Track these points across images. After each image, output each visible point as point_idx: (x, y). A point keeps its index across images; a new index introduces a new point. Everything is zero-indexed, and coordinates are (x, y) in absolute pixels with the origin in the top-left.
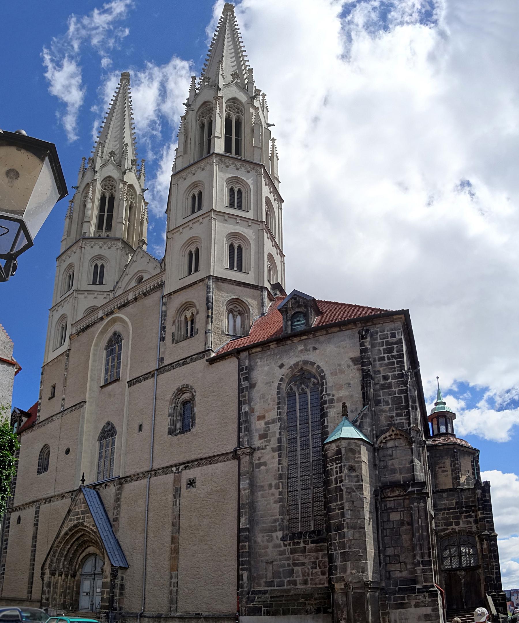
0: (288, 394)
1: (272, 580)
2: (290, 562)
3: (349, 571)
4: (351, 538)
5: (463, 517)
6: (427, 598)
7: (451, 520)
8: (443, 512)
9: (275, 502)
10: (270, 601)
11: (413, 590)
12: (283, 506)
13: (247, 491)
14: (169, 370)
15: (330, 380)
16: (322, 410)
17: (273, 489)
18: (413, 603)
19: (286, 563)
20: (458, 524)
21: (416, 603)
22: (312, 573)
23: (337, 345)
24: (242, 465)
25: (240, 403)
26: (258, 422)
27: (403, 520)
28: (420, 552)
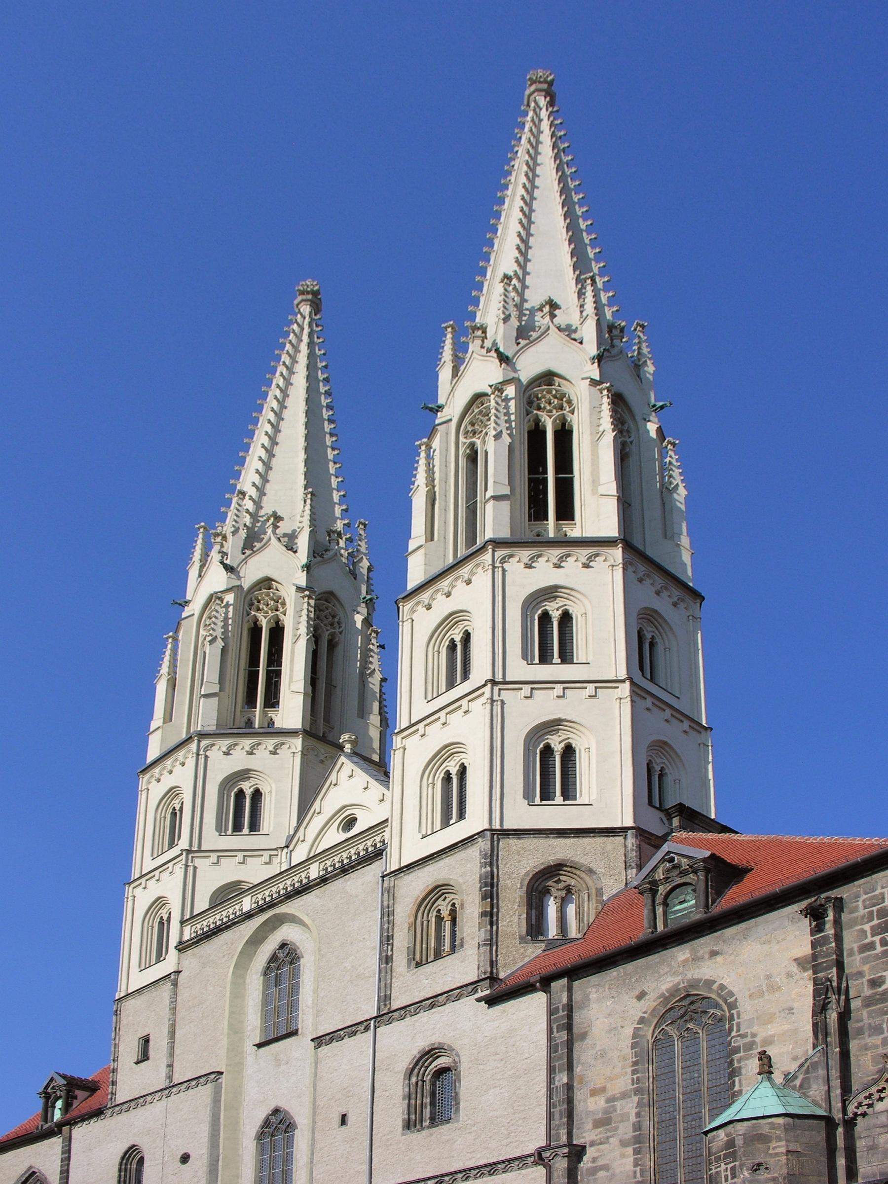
16: (731, 1063)
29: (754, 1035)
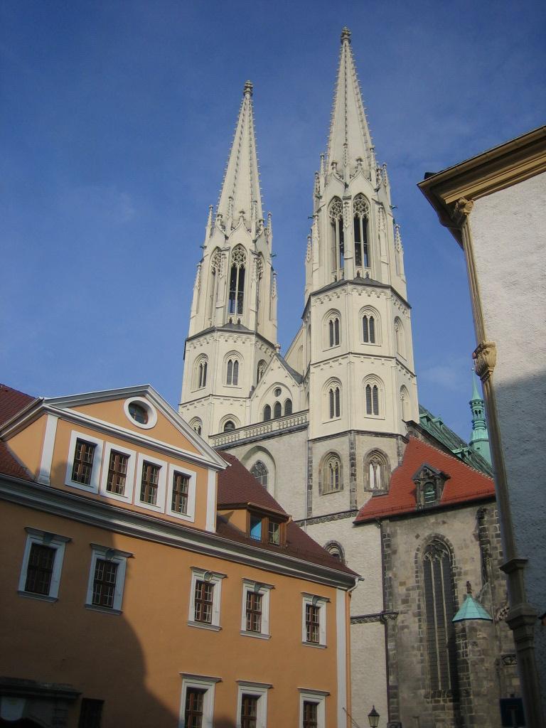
4: (477, 704)
9: (418, 663)
13: (393, 652)
14: (317, 523)
15: (458, 555)
19: (429, 718)
26: (400, 588)
29: (461, 569)
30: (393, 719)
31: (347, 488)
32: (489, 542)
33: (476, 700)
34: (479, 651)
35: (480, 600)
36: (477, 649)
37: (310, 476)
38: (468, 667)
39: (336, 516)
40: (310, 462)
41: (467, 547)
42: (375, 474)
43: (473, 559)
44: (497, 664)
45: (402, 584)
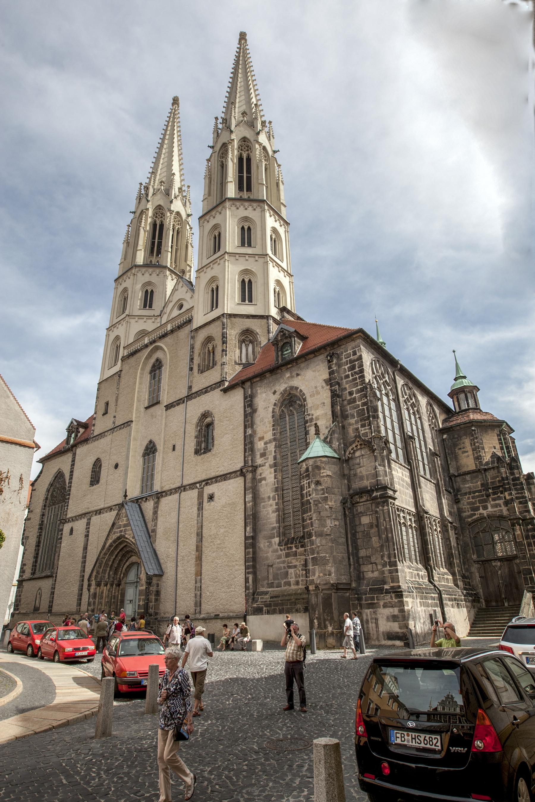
0: (280, 415)
1: (272, 581)
2: (285, 565)
3: (317, 575)
4: (319, 545)
5: (490, 499)
6: (394, 598)
7: (478, 505)
8: (468, 496)
9: (273, 512)
10: (269, 601)
11: (381, 591)
12: (279, 515)
13: (251, 504)
15: (310, 402)
17: (271, 502)
18: (382, 603)
19: (282, 565)
20: (485, 508)
21: (385, 603)
22: (302, 575)
23: (314, 369)
24: (247, 481)
25: (245, 427)
26: (259, 443)
27: (372, 523)
28: (386, 553)
30: (248, 569)
31: (219, 364)
32: (338, 384)
33: (318, 540)
34: (323, 489)
35: (327, 441)
36: (320, 487)
37: (192, 360)
38: (310, 507)
39: (209, 389)
40: (192, 348)
41: (318, 393)
42: (247, 350)
43: (324, 403)
44: (344, 502)
45: (261, 438)
